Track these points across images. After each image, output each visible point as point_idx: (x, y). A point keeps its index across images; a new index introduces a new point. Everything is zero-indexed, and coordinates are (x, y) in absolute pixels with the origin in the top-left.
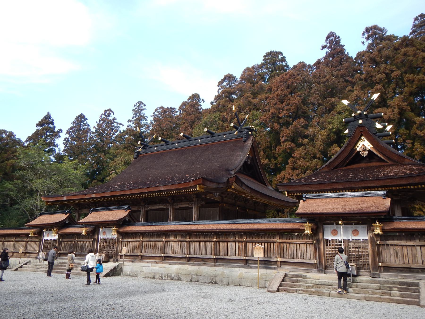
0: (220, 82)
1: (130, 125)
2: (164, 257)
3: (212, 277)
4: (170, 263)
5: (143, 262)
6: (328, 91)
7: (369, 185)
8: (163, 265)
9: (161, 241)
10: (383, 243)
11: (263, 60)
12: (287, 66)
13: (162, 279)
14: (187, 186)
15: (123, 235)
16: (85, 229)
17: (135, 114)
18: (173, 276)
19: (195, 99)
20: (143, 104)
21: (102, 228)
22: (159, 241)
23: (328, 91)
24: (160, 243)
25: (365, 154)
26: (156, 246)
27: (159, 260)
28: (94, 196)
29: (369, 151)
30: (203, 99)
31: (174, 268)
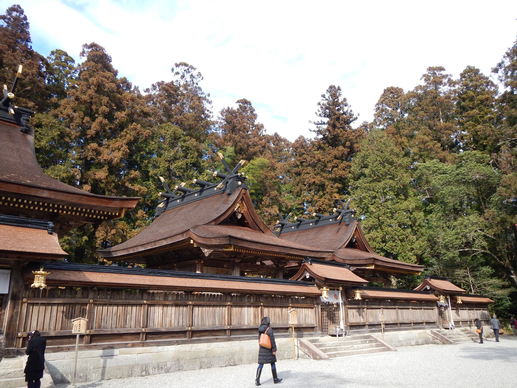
2: (146, 333)
3: (228, 357)
4: (158, 344)
7: (295, 253)
8: (144, 348)
9: (136, 305)
10: (349, 306)
13: (149, 375)
14: (104, 205)
18: (169, 365)
22: (132, 305)
23: (27, 88)
24: (134, 308)
25: (239, 216)
26: (125, 314)
27: (132, 340)
29: (242, 214)
31: (169, 351)
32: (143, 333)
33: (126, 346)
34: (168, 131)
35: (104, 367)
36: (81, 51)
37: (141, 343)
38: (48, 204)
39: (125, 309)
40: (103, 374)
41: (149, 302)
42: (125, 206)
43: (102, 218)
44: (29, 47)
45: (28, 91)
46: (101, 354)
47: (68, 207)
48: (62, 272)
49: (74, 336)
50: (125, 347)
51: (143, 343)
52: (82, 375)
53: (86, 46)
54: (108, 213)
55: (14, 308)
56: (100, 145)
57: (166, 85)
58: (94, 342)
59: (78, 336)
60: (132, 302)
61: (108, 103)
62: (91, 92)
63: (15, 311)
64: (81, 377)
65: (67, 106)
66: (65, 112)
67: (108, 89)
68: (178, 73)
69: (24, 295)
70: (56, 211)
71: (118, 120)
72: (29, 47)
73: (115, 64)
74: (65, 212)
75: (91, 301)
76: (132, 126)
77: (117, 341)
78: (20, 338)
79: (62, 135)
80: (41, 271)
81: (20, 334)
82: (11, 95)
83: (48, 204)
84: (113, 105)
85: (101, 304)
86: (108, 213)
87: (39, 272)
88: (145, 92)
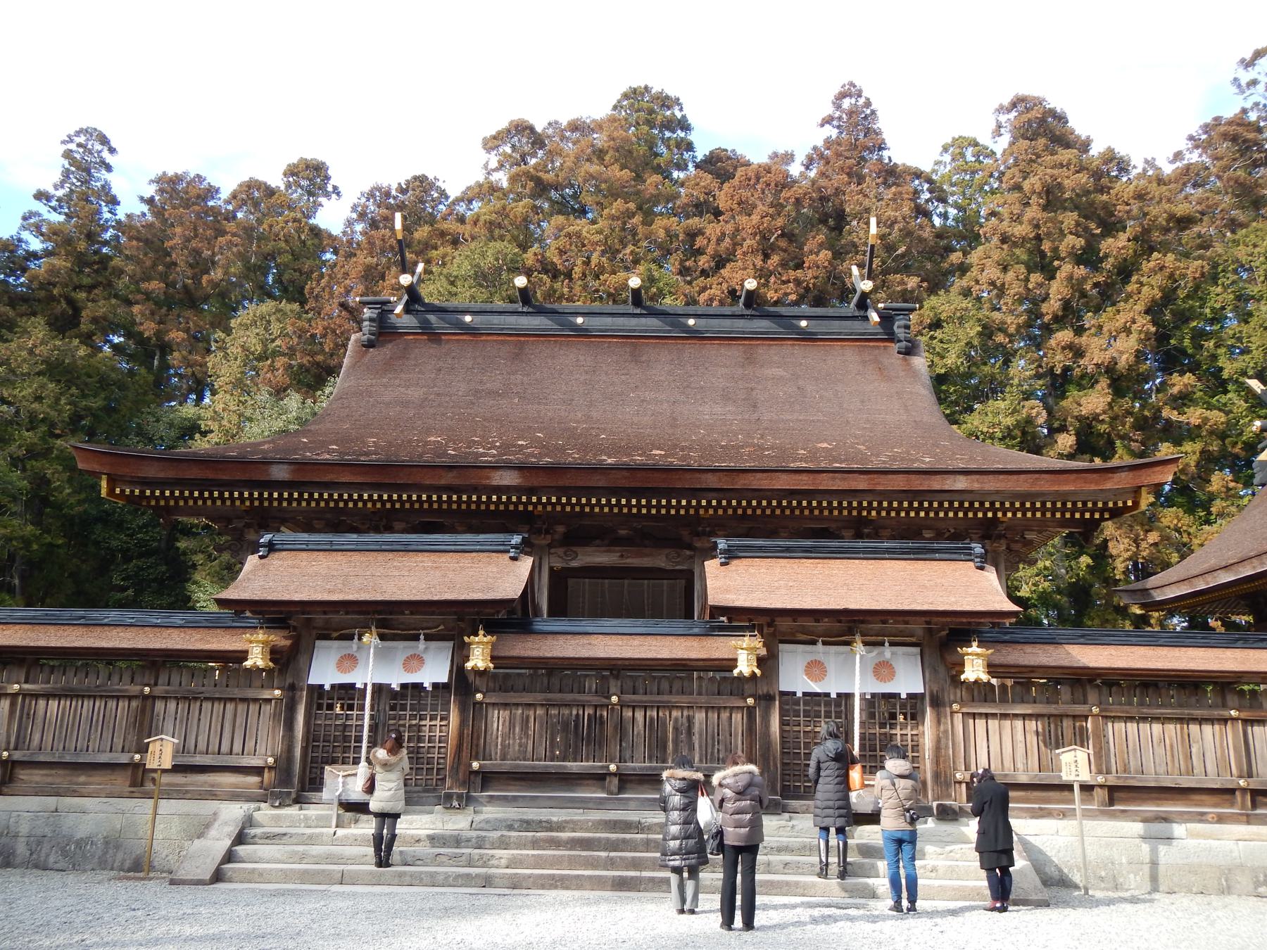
0: (494, 138)
1: (40, 215)
5: (1113, 816)
6: (899, 252)
9: (1211, 721)
11: (615, 108)
12: (690, 147)
14: (1093, 487)
15: (508, 677)
16: (746, 641)
17: (66, 174)
19: (313, 177)
20: (104, 140)
21: (866, 644)
22: (1201, 721)
23: (899, 252)
24: (1207, 729)
27: (1215, 806)
28: (508, 479)
30: (335, 188)
32: (1244, 790)
33: (1201, 817)
34: (1255, 246)
35: (1154, 864)
36: (993, 125)
37: (1241, 814)
38: (971, 504)
39: (1182, 729)
40: (1154, 878)
41: (1244, 715)
42: (1146, 482)
43: (1097, 516)
44: (887, 161)
45: (903, 256)
46: (1142, 833)
47: (1012, 504)
48: (1019, 647)
49: (1068, 787)
50: (1201, 821)
51: (1248, 815)
52: (1103, 874)
53: (1001, 109)
54: (1105, 504)
55: (939, 722)
56: (1080, 331)
57: (1230, 123)
58: (1119, 804)
59: (1076, 788)
60: (1198, 713)
61: (1078, 224)
62: (1034, 212)
63: (942, 728)
64: (1102, 879)
65: (984, 263)
66: (984, 278)
67: (1073, 190)
68: (1254, 83)
69: (952, 698)
70: (990, 515)
71: (1111, 260)
72: (887, 161)
73: (1079, 125)
74: (1009, 515)
75: (1095, 710)
76: (1152, 264)
77: (1175, 805)
78: (960, 783)
79: (988, 331)
80: (975, 648)
81: (959, 776)
82: (867, 285)
83: (971, 504)
84: (1093, 226)
85: (1119, 717)
86: (1105, 504)
87: (970, 650)
88: (1172, 162)
